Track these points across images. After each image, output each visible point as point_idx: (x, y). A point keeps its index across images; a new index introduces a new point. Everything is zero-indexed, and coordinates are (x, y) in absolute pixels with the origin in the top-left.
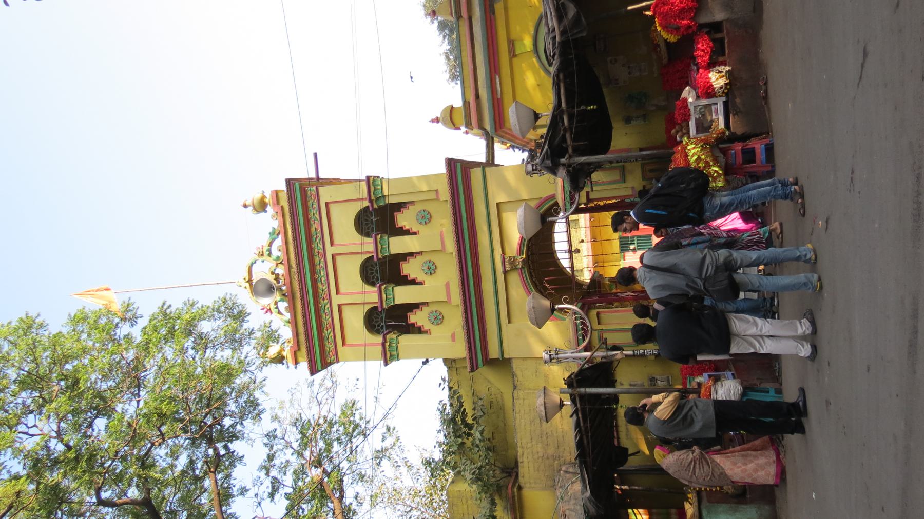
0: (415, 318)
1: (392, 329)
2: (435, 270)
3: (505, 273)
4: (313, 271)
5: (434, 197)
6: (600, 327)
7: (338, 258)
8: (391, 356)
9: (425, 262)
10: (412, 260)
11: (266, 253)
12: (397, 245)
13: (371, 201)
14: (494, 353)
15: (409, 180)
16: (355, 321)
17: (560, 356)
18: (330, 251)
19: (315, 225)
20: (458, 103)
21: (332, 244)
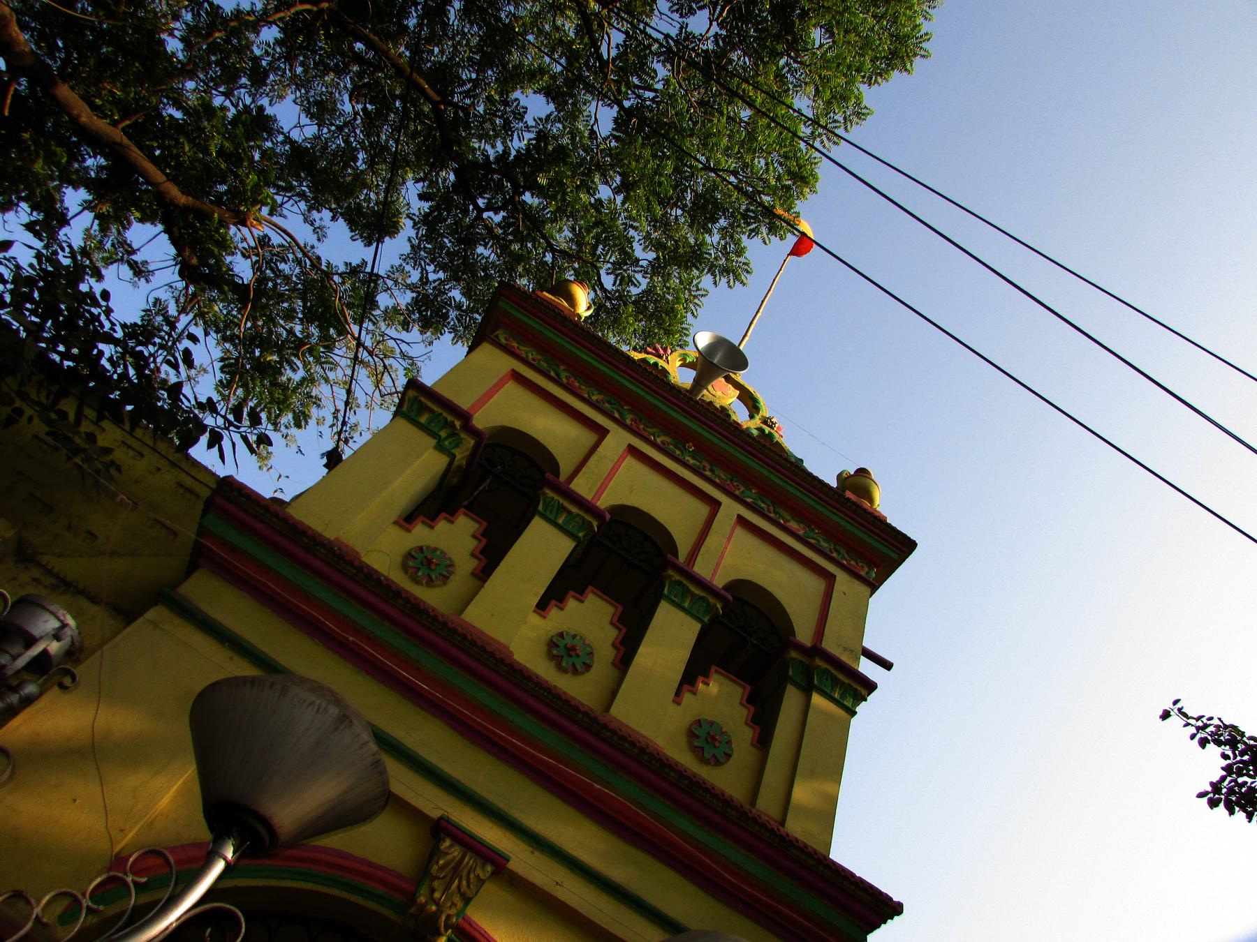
3: (440, 829)
4: (703, 450)
9: (591, 654)
14: (208, 592)
15: (835, 770)
16: (552, 429)
21: (741, 520)
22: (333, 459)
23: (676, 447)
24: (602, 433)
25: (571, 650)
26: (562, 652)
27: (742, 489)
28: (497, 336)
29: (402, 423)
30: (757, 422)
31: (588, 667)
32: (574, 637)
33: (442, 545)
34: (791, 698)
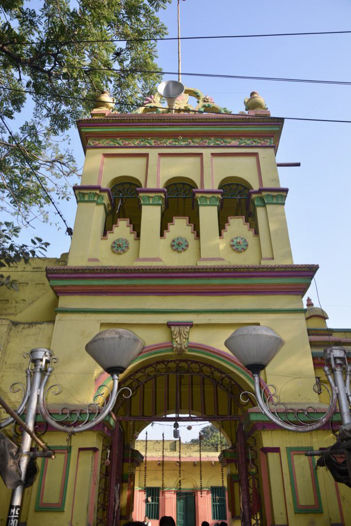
0: (122, 229)
1: (113, 204)
2: (177, 250)
3: (169, 325)
4: (186, 136)
5: (264, 256)
6: (74, 452)
7: (198, 159)
8: (84, 194)
10: (190, 229)
11: (206, 104)
12: (208, 215)
13: (260, 191)
14: (65, 302)
16: (130, 168)
17: (38, 376)
18: (207, 152)
19: (234, 142)
20: (330, 324)
21: (213, 155)
22: (70, 231)
23: (175, 142)
24: (146, 155)
25: (179, 244)
26: (177, 246)
27: (208, 141)
28: (89, 144)
29: (81, 204)
30: (202, 103)
31: (187, 246)
32: (178, 239)
33: (120, 237)
34: (260, 212)
